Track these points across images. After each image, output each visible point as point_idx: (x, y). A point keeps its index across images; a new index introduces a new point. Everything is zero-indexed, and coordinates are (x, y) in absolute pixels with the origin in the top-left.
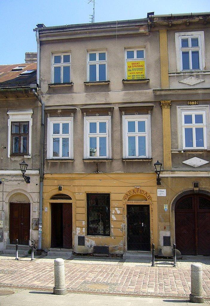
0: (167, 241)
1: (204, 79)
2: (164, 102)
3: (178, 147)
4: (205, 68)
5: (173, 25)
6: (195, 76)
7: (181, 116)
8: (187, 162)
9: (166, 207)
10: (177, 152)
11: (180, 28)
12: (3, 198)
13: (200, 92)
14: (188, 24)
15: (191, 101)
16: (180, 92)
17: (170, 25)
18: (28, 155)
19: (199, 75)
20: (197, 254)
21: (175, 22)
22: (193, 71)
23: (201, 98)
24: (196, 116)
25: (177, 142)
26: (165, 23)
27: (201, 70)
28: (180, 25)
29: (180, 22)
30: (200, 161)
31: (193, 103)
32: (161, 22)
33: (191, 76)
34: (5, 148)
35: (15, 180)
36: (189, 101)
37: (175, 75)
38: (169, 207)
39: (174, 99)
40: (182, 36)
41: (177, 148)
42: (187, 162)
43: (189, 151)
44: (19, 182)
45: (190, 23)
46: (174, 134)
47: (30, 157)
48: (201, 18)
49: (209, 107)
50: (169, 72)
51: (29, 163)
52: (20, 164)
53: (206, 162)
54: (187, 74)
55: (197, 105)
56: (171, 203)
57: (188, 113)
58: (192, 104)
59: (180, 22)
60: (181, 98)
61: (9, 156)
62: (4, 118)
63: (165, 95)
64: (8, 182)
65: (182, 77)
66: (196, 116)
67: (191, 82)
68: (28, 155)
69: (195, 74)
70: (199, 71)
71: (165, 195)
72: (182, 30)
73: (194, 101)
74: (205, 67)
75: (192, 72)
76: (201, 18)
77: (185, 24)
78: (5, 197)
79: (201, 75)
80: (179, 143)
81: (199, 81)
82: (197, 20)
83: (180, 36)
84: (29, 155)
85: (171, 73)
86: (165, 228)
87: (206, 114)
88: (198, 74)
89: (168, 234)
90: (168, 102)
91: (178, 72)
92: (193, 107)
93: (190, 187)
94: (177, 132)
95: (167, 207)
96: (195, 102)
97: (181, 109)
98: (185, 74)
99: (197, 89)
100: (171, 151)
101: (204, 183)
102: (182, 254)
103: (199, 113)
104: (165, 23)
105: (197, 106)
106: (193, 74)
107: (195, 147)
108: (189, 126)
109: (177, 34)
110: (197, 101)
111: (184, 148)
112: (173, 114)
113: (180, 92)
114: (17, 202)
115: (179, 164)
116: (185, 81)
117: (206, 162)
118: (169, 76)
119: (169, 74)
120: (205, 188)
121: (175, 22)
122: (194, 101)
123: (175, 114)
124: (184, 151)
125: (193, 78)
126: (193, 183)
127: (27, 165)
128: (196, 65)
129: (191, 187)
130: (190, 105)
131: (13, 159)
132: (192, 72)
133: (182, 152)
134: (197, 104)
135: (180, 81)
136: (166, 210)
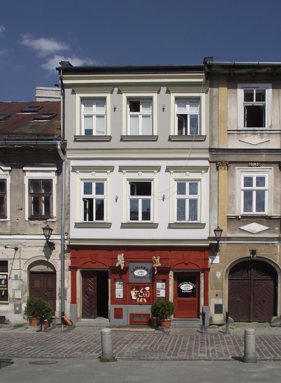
0: (218, 309)
1: (269, 138)
3: (235, 212)
4: (271, 127)
5: (236, 75)
7: (240, 178)
8: (245, 228)
9: (219, 275)
12: (20, 266)
14: (254, 74)
15: (253, 162)
17: (232, 75)
18: (52, 218)
20: (252, 321)
21: (238, 71)
24: (258, 178)
26: (226, 71)
29: (244, 71)
30: (260, 227)
31: (255, 164)
32: (221, 71)
34: (21, 209)
35: (35, 246)
37: (236, 132)
38: (222, 274)
41: (234, 212)
42: (245, 228)
45: (257, 74)
46: (232, 198)
47: (55, 220)
48: (269, 69)
49: (273, 169)
50: (229, 129)
51: (54, 227)
52: (43, 229)
53: (267, 228)
55: (259, 166)
56: (225, 271)
58: (254, 165)
59: (244, 71)
61: (27, 219)
62: (19, 175)
64: (26, 248)
66: (258, 178)
73: (256, 162)
74: (271, 124)
76: (269, 69)
77: (250, 74)
78: (22, 265)
80: (237, 208)
82: (264, 70)
86: (217, 295)
87: (269, 176)
89: (220, 302)
92: (255, 169)
93: (246, 254)
95: (220, 275)
101: (263, 249)
102: (234, 322)
103: (261, 175)
104: (226, 71)
105: (259, 168)
106: (256, 132)
107: (254, 212)
110: (259, 162)
111: (242, 212)
112: (232, 176)
115: (235, 230)
117: (267, 228)
119: (228, 131)
120: (263, 255)
121: (238, 71)
122: (256, 162)
123: (233, 176)
127: (52, 230)
129: (248, 254)
131: (32, 222)
135: (240, 140)
136: (218, 277)
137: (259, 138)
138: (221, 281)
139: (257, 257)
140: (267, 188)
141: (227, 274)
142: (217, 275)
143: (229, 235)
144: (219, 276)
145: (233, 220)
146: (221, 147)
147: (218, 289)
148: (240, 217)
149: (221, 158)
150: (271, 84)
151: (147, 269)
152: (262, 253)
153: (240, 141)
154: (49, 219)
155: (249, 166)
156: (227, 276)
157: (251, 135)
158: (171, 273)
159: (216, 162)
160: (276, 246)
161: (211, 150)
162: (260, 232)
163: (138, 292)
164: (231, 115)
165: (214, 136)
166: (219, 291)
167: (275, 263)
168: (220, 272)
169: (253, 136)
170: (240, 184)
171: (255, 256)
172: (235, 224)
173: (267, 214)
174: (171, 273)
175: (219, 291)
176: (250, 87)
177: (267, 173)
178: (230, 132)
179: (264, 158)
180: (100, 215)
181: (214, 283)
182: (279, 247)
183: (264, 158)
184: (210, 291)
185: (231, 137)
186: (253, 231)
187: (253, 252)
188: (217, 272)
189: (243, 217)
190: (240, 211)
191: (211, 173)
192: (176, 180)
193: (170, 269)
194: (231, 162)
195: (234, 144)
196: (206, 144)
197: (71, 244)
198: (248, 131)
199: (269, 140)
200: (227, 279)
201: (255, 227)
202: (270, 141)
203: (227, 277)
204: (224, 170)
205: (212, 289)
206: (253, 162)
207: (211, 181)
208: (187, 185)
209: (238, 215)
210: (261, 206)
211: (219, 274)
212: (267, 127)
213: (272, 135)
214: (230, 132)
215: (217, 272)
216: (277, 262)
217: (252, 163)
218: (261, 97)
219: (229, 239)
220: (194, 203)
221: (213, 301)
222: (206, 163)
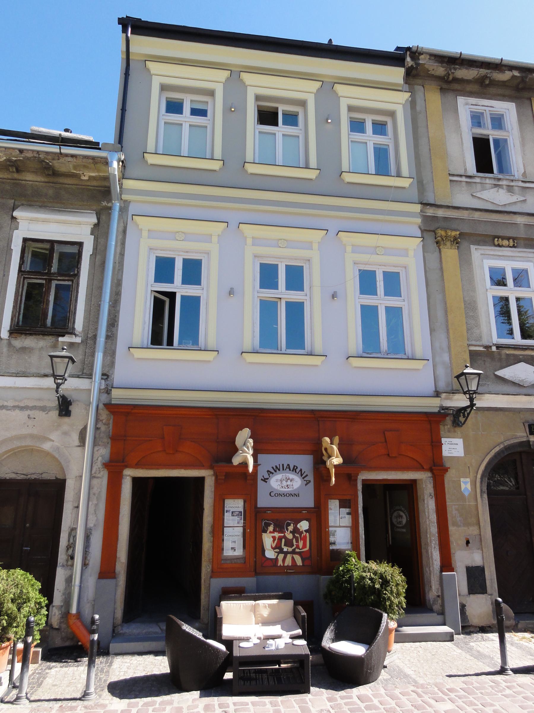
1: (524, 196)
2: (443, 233)
3: (481, 337)
6: (505, 187)
7: (482, 268)
9: (466, 485)
10: (481, 349)
11: (469, 88)
13: (520, 220)
15: (503, 238)
16: (477, 215)
18: (72, 333)
19: (513, 186)
22: (500, 176)
23: (522, 234)
25: (478, 326)
27: (516, 176)
28: (468, 82)
31: (505, 242)
33: (496, 186)
36: (498, 237)
37: (464, 179)
38: (474, 484)
39: (466, 229)
40: (472, 105)
41: (480, 338)
42: (506, 373)
43: (508, 347)
44: (31, 413)
47: (78, 340)
54: (488, 181)
56: (479, 476)
57: (498, 264)
58: (504, 244)
60: (482, 230)
63: (446, 219)
65: (479, 186)
68: (72, 333)
69: (504, 183)
70: (512, 178)
71: (462, 455)
72: (471, 94)
73: (508, 239)
74: (525, 172)
75: (499, 179)
79: (516, 188)
83: (467, 104)
84: (76, 335)
85: (453, 175)
86: (468, 542)
88: (512, 184)
90: (454, 233)
94: (475, 302)
95: (469, 486)
96: (511, 241)
97: (482, 252)
98: (484, 181)
99: (515, 213)
100: (469, 345)
103: (520, 265)
108: (501, 292)
109: (461, 100)
110: (514, 239)
111: (495, 340)
113: (477, 215)
114: (13, 476)
116: (485, 195)
118: (451, 181)
122: (508, 239)
124: (498, 347)
125: (501, 190)
126: (527, 425)
130: (499, 246)
132: (499, 179)
133: (494, 349)
134: (514, 246)
135: (474, 194)
136: (466, 494)
137: (506, 193)
138: (473, 503)
141: (483, 483)
142: (463, 486)
144: (466, 488)
147: (467, 524)
151: (301, 470)
153: (472, 195)
154: (63, 336)
156: (483, 490)
157: (492, 188)
163: (279, 536)
165: (424, 182)
166: (473, 531)
168: (468, 480)
169: (496, 189)
172: (484, 364)
175: (473, 531)
176: (479, 105)
177: (531, 261)
181: (457, 507)
186: (522, 380)
188: (462, 480)
191: (425, 254)
199: (526, 200)
202: (528, 201)
203: (484, 492)
204: (451, 248)
207: (427, 269)
211: (465, 483)
213: (528, 190)
215: (462, 480)
217: (500, 239)
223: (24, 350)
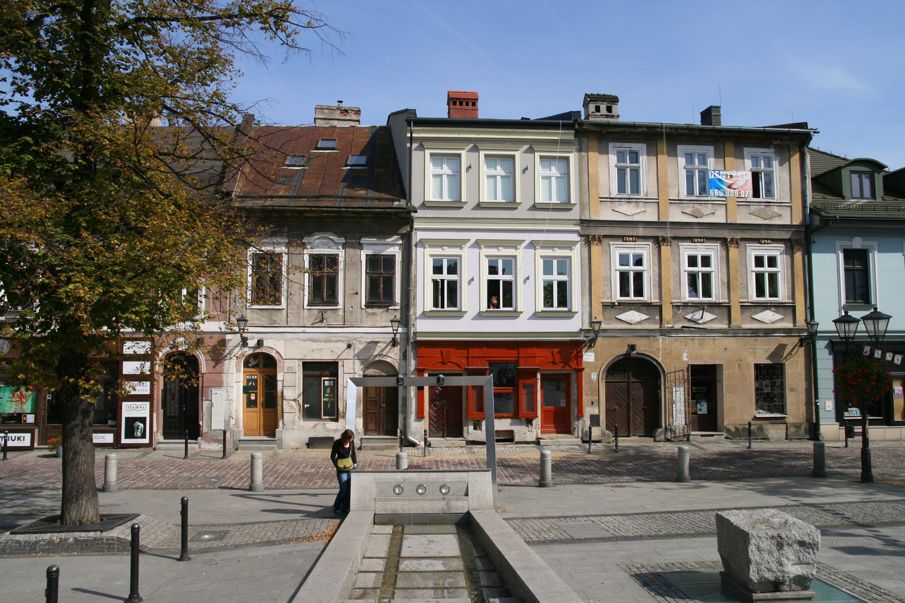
4: (647, 194)
7: (615, 255)
8: (620, 317)
9: (594, 376)
36: (626, 236)
42: (622, 316)
53: (646, 317)
67: (627, 212)
81: (639, 211)
83: (615, 147)
86: (592, 403)
89: (595, 411)
91: (612, 196)
95: (595, 377)
115: (611, 319)
117: (646, 317)
128: (636, 188)
139: (637, 353)
140: (645, 268)
143: (604, 326)
145: (609, 306)
146: (594, 218)
147: (593, 395)
148: (616, 304)
149: (593, 231)
150: (645, 145)
152: (643, 347)
155: (623, 241)
158: (539, 376)
159: (587, 236)
160: (658, 340)
161: (582, 222)
162: (639, 323)
164: (603, 179)
167: (657, 362)
169: (628, 205)
170: (615, 263)
171: (635, 352)
173: (646, 299)
174: (539, 376)
178: (603, 200)
179: (641, 231)
180: (453, 302)
182: (661, 340)
183: (641, 231)
184: (585, 398)
185: (604, 205)
187: (632, 348)
189: (620, 304)
190: (617, 297)
192: (542, 257)
193: (537, 370)
194: (605, 236)
195: (606, 214)
196: (575, 214)
197: (418, 339)
198: (622, 198)
200: (604, 381)
201: (633, 316)
205: (586, 395)
206: (629, 236)
208: (555, 262)
209: (613, 301)
210: (639, 292)
212: (642, 195)
214: (603, 200)
216: (660, 360)
218: (635, 157)
219: (605, 330)
220: (562, 286)
221: (589, 411)
222: (575, 237)
223: (373, 314)
